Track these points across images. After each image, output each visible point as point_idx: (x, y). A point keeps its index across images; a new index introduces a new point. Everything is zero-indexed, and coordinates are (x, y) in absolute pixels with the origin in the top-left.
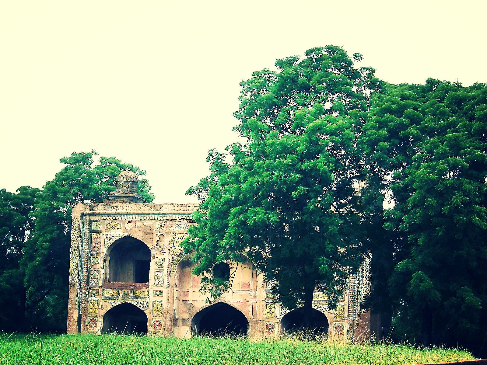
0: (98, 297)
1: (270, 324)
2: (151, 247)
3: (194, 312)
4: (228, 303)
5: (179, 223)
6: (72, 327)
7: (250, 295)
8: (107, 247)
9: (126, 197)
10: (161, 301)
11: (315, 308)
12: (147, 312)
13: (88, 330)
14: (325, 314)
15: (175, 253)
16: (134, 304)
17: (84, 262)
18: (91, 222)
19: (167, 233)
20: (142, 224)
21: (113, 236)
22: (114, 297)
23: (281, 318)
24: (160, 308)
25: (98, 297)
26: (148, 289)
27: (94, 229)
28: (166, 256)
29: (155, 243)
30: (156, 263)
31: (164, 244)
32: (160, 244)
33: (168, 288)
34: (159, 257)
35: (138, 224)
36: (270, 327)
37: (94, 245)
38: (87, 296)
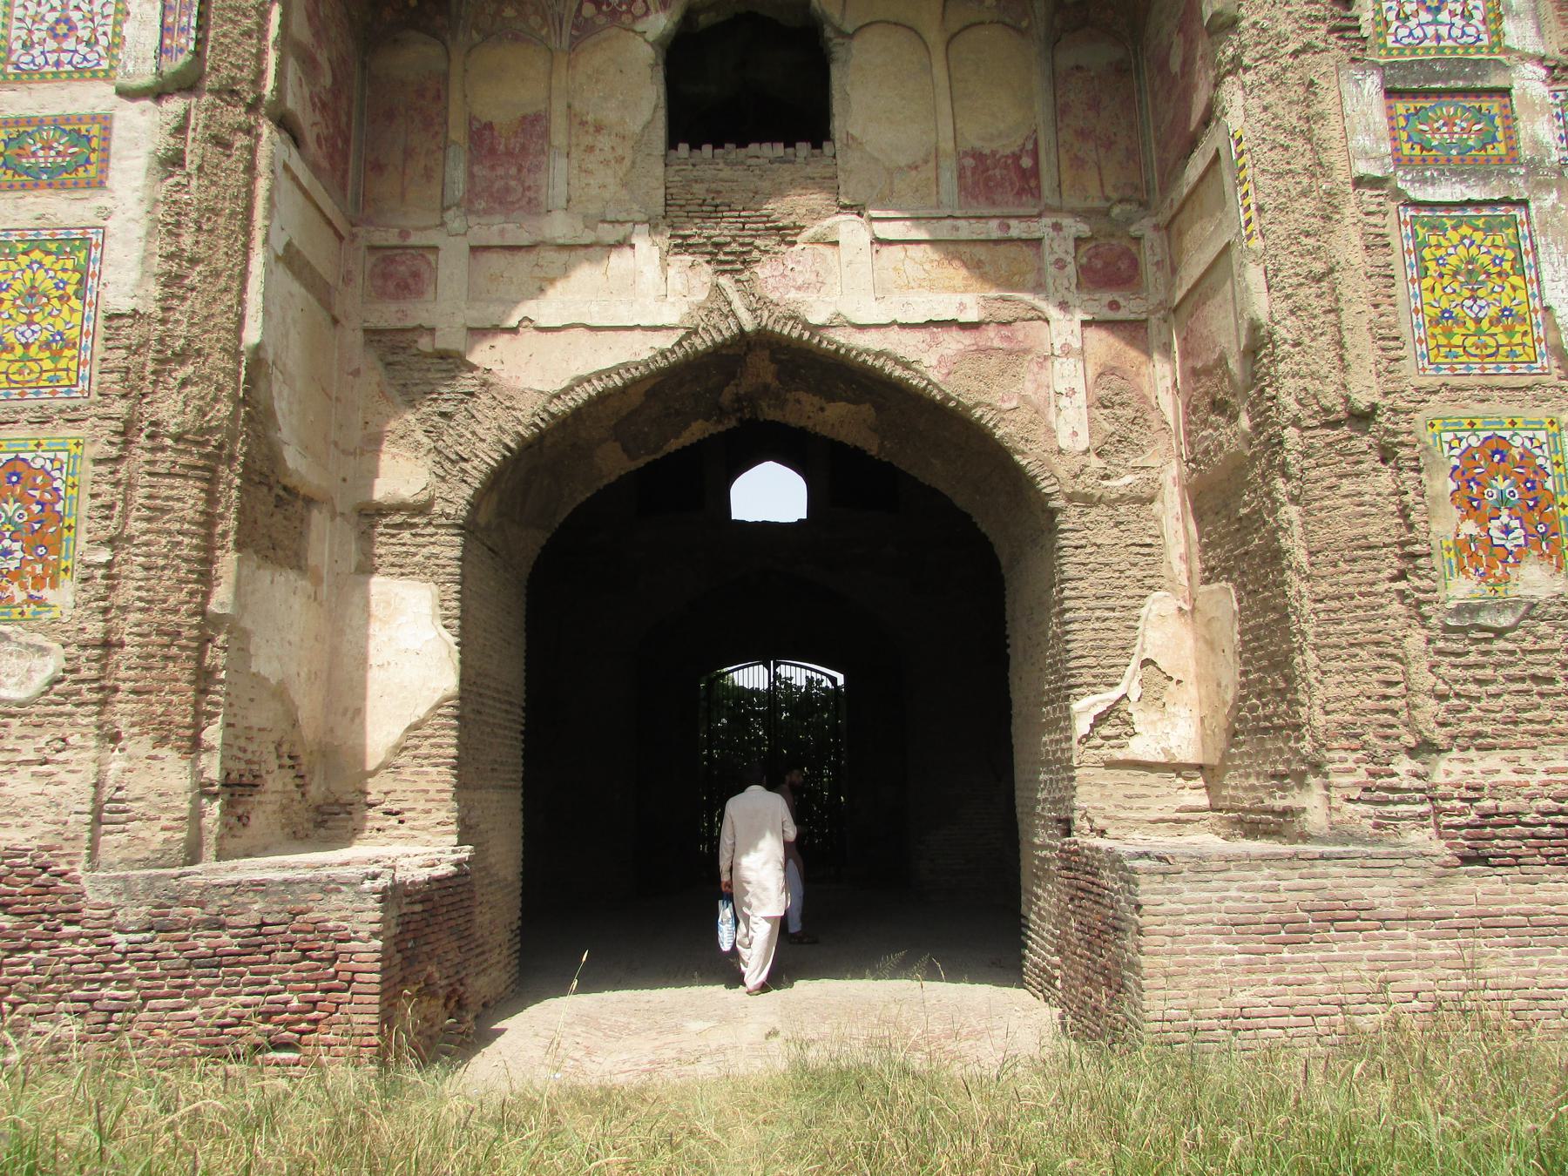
1: (1497, 449)
4: (841, 337)
7: (1049, 259)
24: (68, 319)
33: (175, 105)
36: (1502, 484)
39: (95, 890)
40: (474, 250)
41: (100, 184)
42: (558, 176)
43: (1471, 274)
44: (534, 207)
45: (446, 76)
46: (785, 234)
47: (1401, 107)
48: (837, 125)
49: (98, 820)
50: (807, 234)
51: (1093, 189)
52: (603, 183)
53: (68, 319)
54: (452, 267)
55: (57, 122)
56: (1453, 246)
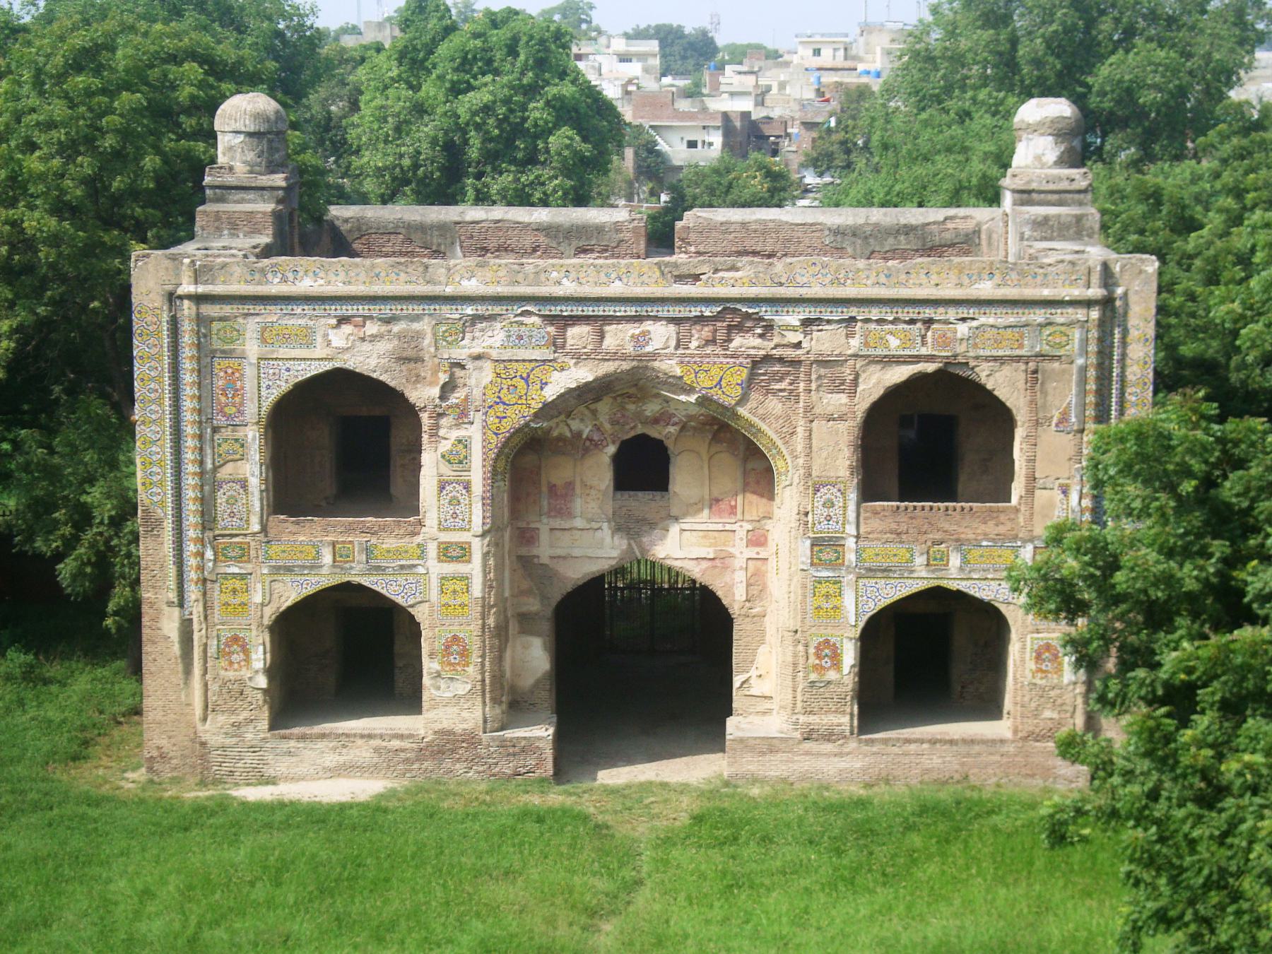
0: (249, 567)
1: (827, 641)
2: (420, 404)
3: (557, 595)
5: (515, 328)
6: (161, 661)
8: (267, 404)
9: (263, 189)
10: (466, 578)
11: (972, 593)
12: (421, 614)
13: (222, 673)
14: (1003, 608)
15: (508, 426)
16: (374, 587)
17: (189, 455)
18: (200, 320)
19: (478, 357)
20: (384, 328)
21: (288, 370)
22: (304, 567)
23: (861, 625)
24: (465, 598)
25: (249, 567)
26: (418, 539)
27: (217, 344)
28: (474, 433)
29: (436, 391)
30: (443, 456)
31: (467, 396)
32: (455, 398)
34: (455, 434)
35: (372, 328)
37: (223, 399)
38: (211, 564)
39: (485, 737)
40: (552, 529)
41: (469, 561)
42: (578, 504)
43: (827, 596)
44: (570, 515)
45: (539, 468)
46: (652, 525)
47: (816, 549)
48: (670, 487)
49: (485, 721)
50: (660, 526)
51: (754, 513)
52: (593, 507)
53: (465, 598)
54: (544, 536)
55: (456, 543)
56: (823, 589)
